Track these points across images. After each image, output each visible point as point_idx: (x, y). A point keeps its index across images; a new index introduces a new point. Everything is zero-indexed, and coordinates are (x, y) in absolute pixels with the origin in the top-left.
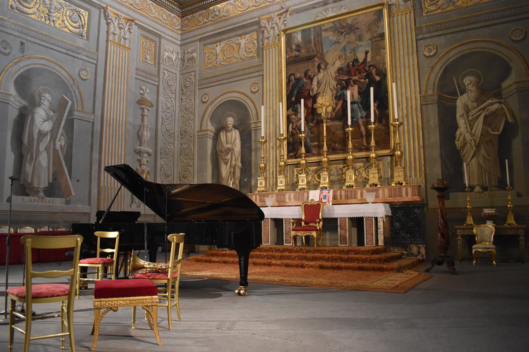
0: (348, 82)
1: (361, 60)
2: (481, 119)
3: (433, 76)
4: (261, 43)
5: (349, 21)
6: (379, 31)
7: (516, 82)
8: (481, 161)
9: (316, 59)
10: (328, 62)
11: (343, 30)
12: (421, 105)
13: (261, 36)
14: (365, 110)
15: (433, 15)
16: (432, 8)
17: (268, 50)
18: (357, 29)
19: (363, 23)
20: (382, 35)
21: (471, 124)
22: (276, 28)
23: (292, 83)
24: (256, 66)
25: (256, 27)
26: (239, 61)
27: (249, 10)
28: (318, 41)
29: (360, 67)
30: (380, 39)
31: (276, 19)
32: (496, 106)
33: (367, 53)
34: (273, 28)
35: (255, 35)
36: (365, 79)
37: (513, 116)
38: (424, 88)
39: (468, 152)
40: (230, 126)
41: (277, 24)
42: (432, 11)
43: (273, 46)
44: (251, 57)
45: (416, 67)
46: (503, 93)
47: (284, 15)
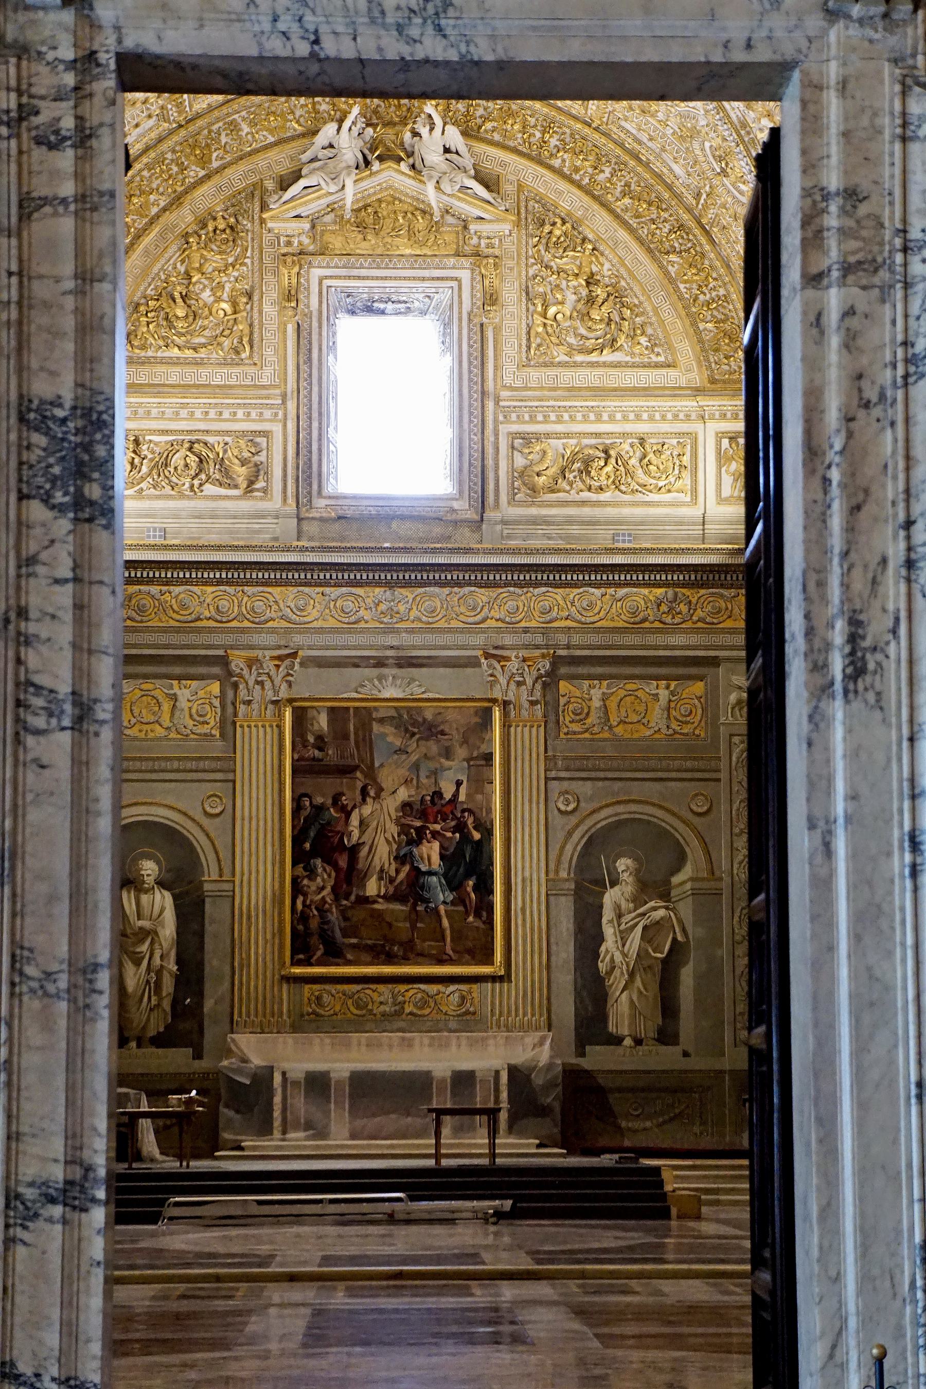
0: (420, 831)
1: (448, 796)
2: (639, 929)
3: (569, 848)
4: (230, 710)
5: (429, 715)
6: (484, 748)
7: (692, 879)
8: (635, 998)
9: (358, 774)
10: (384, 785)
11: (416, 730)
12: (547, 895)
13: (230, 693)
14: (451, 890)
15: (578, 740)
16: (575, 727)
17: (246, 729)
18: (443, 733)
19: (455, 726)
20: (489, 757)
21: (623, 936)
22: (268, 685)
23: (304, 814)
24: (218, 759)
25: (216, 670)
26: (173, 735)
27: (198, 624)
28: (364, 740)
29: (444, 809)
30: (483, 762)
31: (269, 666)
32: (661, 913)
33: (459, 784)
34: (261, 683)
35: (215, 688)
36: (453, 833)
37: (684, 930)
38: (552, 866)
39: (616, 982)
40: (150, 881)
41: (270, 677)
42: (575, 733)
43: (260, 724)
44: (205, 735)
45: (542, 828)
46: (673, 893)
47: (287, 662)
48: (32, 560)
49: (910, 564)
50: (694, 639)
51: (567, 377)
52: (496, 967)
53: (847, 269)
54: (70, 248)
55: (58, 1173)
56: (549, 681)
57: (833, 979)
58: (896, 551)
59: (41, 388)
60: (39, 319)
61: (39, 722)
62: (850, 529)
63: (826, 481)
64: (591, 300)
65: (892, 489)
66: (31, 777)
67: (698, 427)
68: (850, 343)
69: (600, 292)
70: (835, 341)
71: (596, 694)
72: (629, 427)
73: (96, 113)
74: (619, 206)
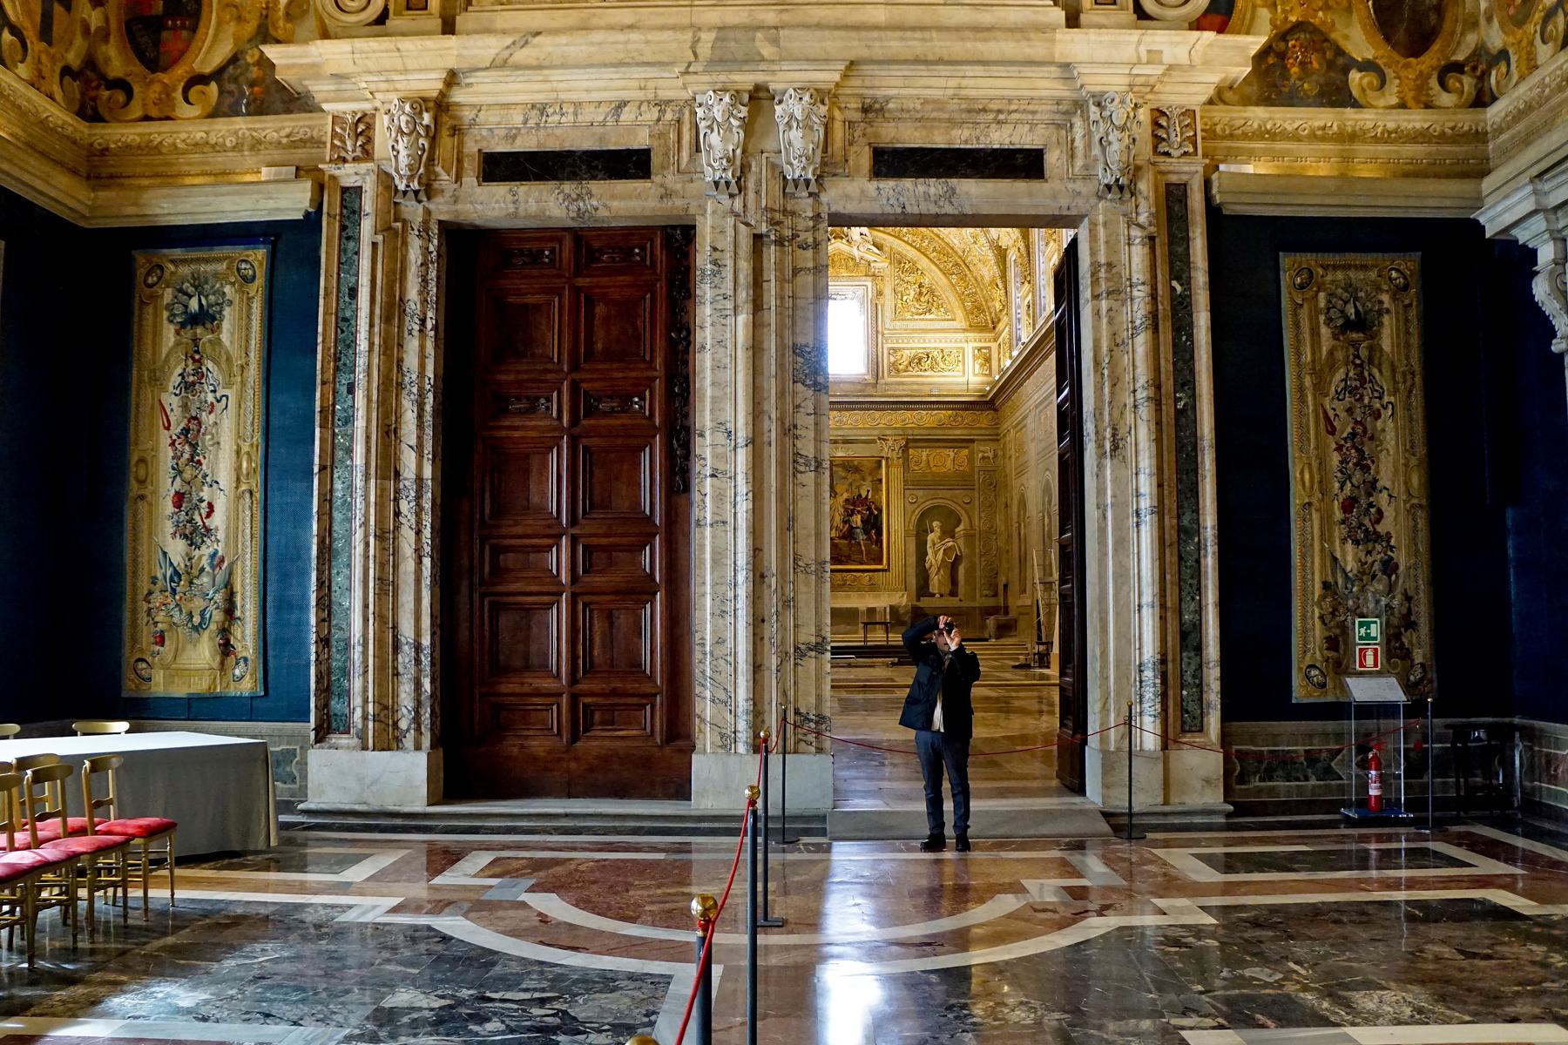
0: (853, 511)
2: (942, 551)
20: (880, 481)
39: (933, 572)
48: (798, 406)
49: (1135, 406)
50: (964, 432)
51: (911, 325)
52: (884, 565)
53: (1109, 293)
54: (811, 287)
55: (813, 640)
56: (905, 448)
57: (1106, 566)
58: (1130, 401)
59: (800, 340)
60: (799, 313)
61: (802, 468)
62: (1112, 393)
63: (1103, 374)
64: (921, 294)
65: (1128, 377)
66: (800, 490)
67: (965, 345)
68: (1110, 322)
69: (924, 290)
70: (1105, 321)
71: (924, 454)
72: (937, 345)
73: (820, 236)
74: (931, 256)
